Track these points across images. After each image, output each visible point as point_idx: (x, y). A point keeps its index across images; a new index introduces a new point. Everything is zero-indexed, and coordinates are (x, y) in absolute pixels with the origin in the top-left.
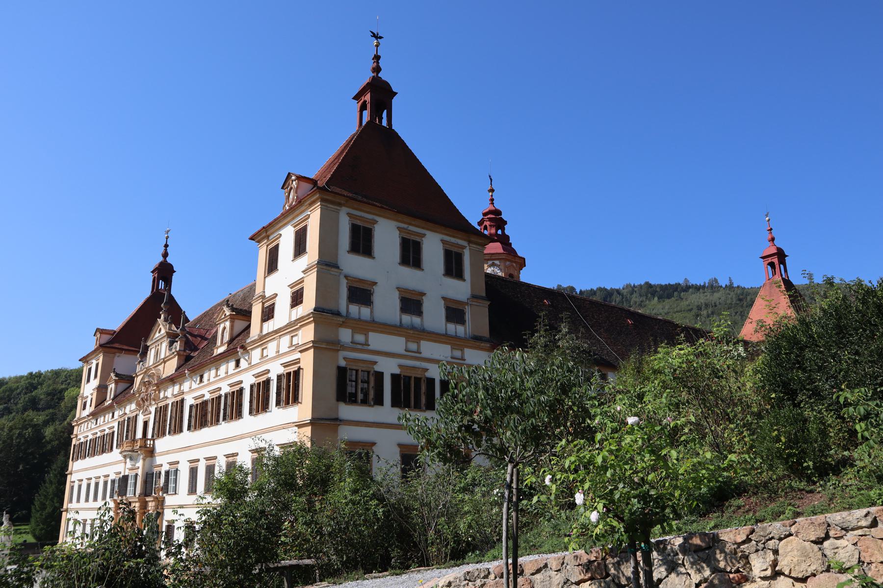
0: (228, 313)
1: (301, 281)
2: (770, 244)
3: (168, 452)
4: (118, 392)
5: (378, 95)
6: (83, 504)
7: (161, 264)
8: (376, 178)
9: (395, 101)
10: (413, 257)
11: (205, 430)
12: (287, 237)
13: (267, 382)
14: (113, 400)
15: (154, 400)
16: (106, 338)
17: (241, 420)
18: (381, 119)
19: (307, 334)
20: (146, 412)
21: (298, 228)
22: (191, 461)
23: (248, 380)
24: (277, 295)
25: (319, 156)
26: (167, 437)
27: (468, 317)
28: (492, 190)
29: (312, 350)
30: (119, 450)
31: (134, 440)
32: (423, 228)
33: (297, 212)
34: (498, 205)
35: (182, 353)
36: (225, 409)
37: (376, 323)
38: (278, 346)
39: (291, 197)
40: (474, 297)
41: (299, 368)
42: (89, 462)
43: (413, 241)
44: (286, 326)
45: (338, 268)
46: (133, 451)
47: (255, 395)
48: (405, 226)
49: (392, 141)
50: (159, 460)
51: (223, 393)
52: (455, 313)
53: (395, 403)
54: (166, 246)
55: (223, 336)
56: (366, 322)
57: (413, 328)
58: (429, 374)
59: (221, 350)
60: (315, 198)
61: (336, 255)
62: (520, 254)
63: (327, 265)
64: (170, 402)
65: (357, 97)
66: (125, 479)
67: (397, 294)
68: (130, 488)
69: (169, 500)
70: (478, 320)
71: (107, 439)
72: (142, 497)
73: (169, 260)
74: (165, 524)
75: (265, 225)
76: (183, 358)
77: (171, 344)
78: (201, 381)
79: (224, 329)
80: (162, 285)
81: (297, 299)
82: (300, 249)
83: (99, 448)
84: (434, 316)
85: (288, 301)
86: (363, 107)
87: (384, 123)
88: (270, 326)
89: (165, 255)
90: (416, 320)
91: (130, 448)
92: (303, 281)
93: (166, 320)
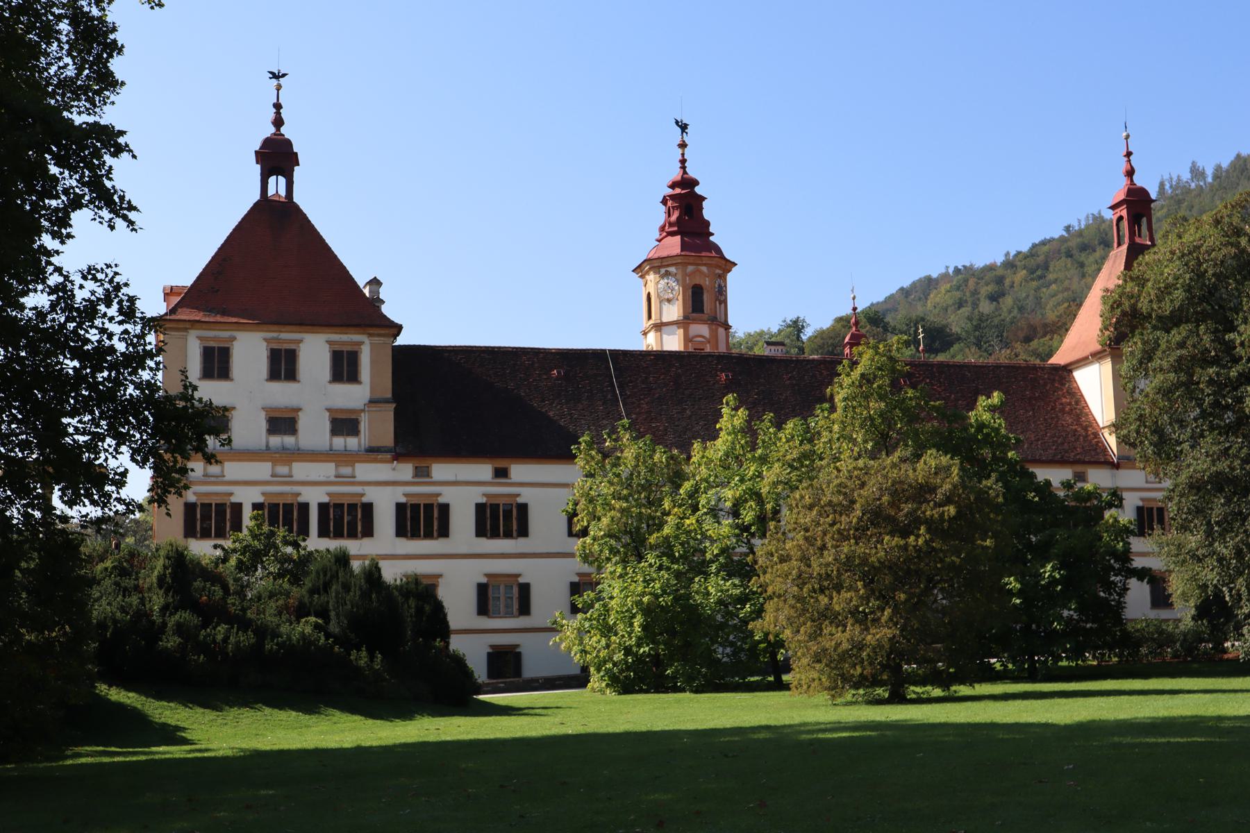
5: (277, 157)
27: (363, 426)
34: (692, 172)
43: (286, 350)
48: (275, 335)
52: (344, 424)
67: (263, 415)
70: (379, 427)
84: (314, 431)
90: (289, 440)
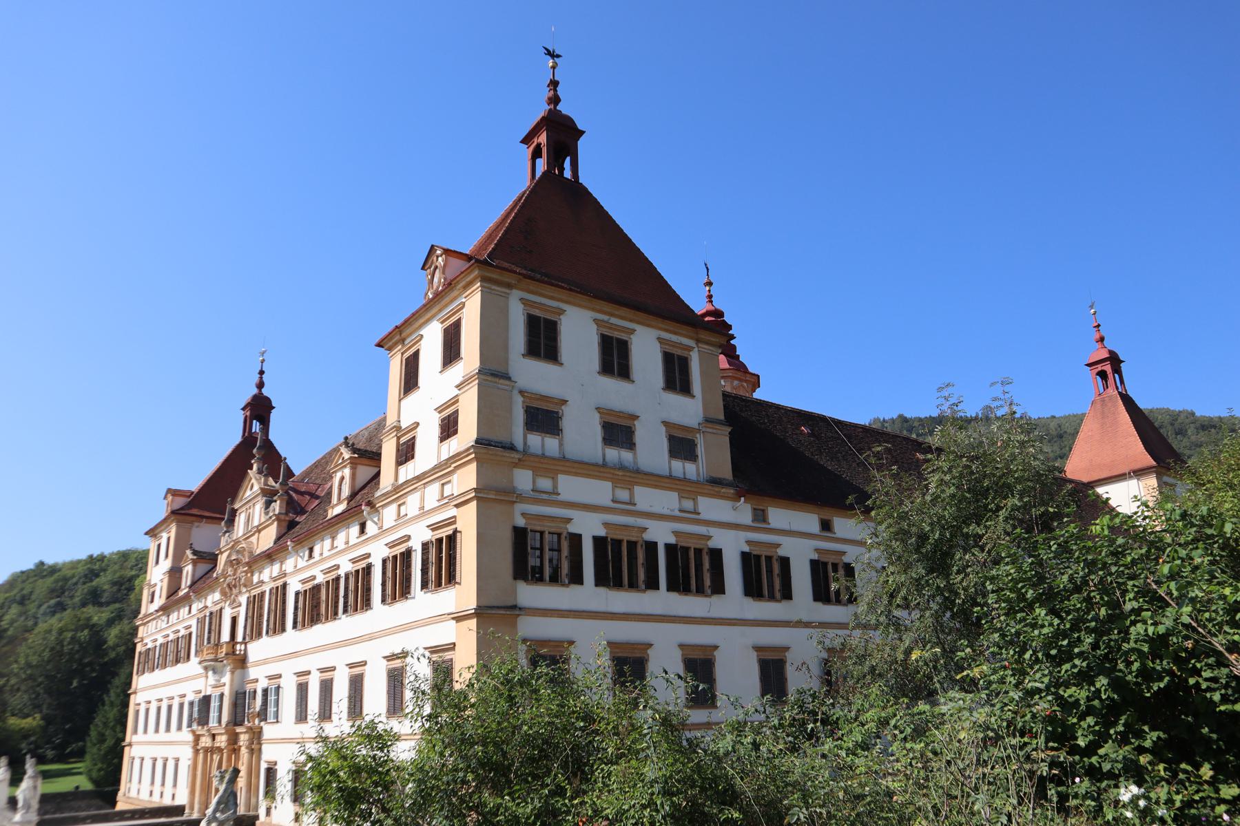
0: (347, 454)
1: (454, 400)
2: (1098, 345)
3: (265, 662)
4: (198, 574)
5: (559, 135)
6: (151, 735)
7: (255, 398)
8: (558, 247)
9: (582, 143)
10: (619, 364)
11: (318, 628)
12: (431, 338)
13: (407, 554)
14: (190, 587)
15: (245, 586)
16: (180, 502)
17: (369, 612)
18: (562, 169)
19: (466, 479)
20: (235, 604)
21: (448, 323)
22: (299, 674)
23: (378, 552)
24: (418, 424)
25: (477, 218)
26: (265, 639)
27: (700, 450)
28: (710, 284)
29: (474, 503)
30: (198, 660)
31: (218, 645)
32: (631, 321)
33: (447, 299)
34: (718, 304)
35: (283, 517)
36: (346, 596)
37: (568, 460)
38: (422, 499)
39: (436, 280)
40: (708, 420)
41: (456, 531)
42: (159, 676)
44: (434, 468)
45: (509, 379)
46: (216, 660)
47: (389, 574)
48: (605, 318)
49: (579, 198)
50: (253, 673)
51: (342, 572)
52: (681, 446)
53: (601, 581)
54: (262, 372)
55: (340, 489)
56: (554, 459)
57: (622, 467)
58: (648, 536)
59: (338, 510)
60: (472, 276)
61: (506, 360)
62: (751, 370)
63: (492, 375)
64: (267, 588)
65: (526, 140)
66: (206, 700)
68: (213, 714)
69: (269, 731)
70: (715, 454)
71: (182, 644)
72: (230, 727)
73: (265, 392)
74: (264, 766)
75: (398, 323)
76: (285, 524)
77: (268, 504)
78: (311, 556)
79: (342, 480)
80: (256, 427)
81: (449, 428)
82: (451, 352)
83: (170, 657)
84: (651, 450)
85: (436, 431)
86: (537, 154)
87: (568, 174)
88: (409, 471)
89: (261, 385)
90: (626, 456)
91: (212, 657)
92: (457, 401)
93: (260, 472)
